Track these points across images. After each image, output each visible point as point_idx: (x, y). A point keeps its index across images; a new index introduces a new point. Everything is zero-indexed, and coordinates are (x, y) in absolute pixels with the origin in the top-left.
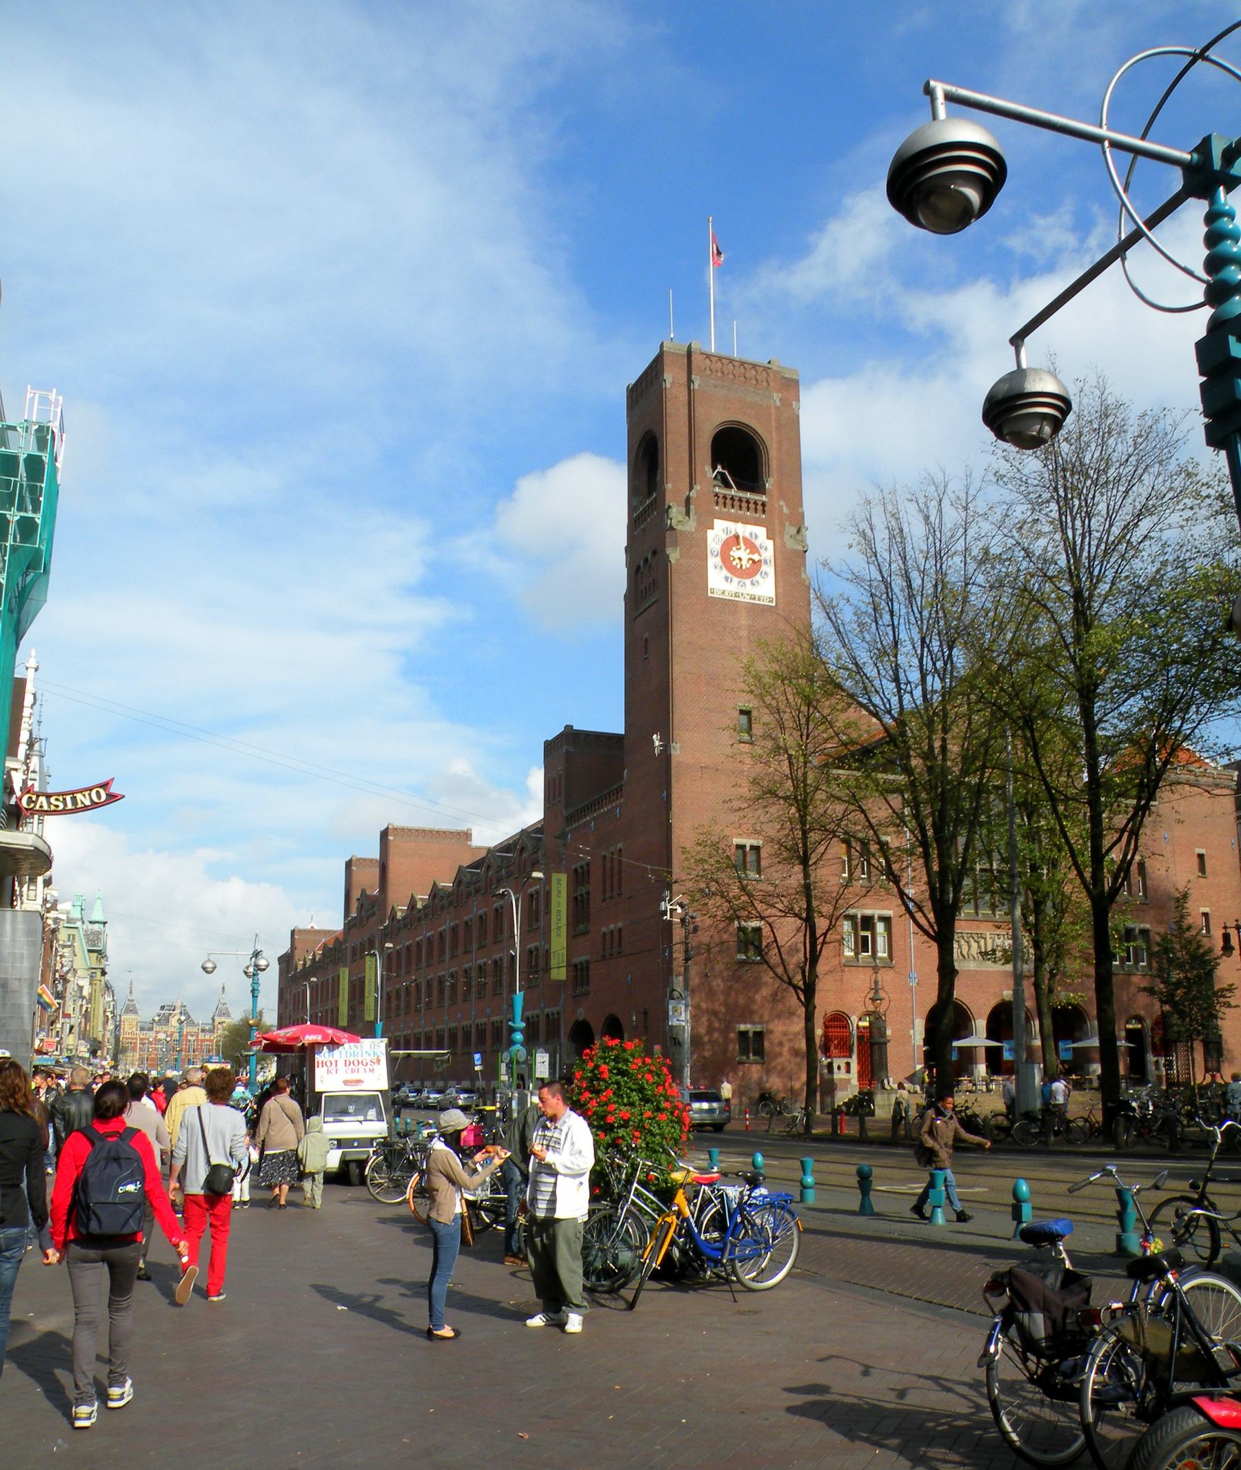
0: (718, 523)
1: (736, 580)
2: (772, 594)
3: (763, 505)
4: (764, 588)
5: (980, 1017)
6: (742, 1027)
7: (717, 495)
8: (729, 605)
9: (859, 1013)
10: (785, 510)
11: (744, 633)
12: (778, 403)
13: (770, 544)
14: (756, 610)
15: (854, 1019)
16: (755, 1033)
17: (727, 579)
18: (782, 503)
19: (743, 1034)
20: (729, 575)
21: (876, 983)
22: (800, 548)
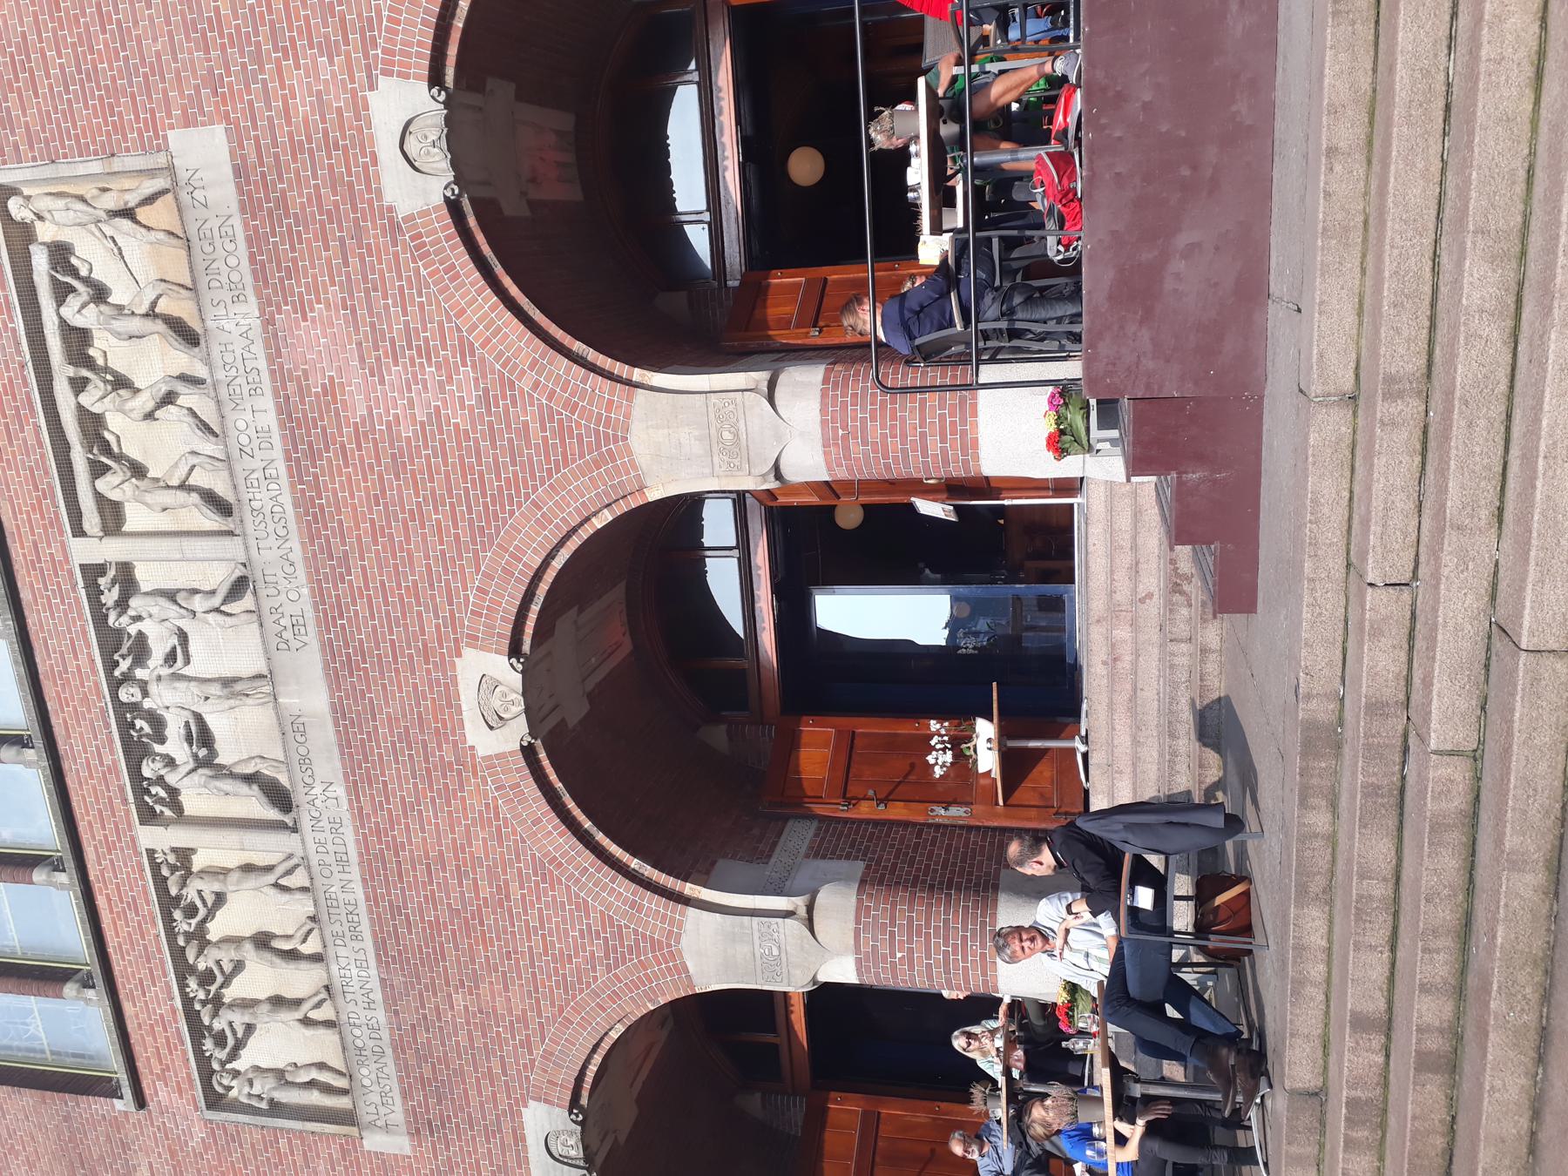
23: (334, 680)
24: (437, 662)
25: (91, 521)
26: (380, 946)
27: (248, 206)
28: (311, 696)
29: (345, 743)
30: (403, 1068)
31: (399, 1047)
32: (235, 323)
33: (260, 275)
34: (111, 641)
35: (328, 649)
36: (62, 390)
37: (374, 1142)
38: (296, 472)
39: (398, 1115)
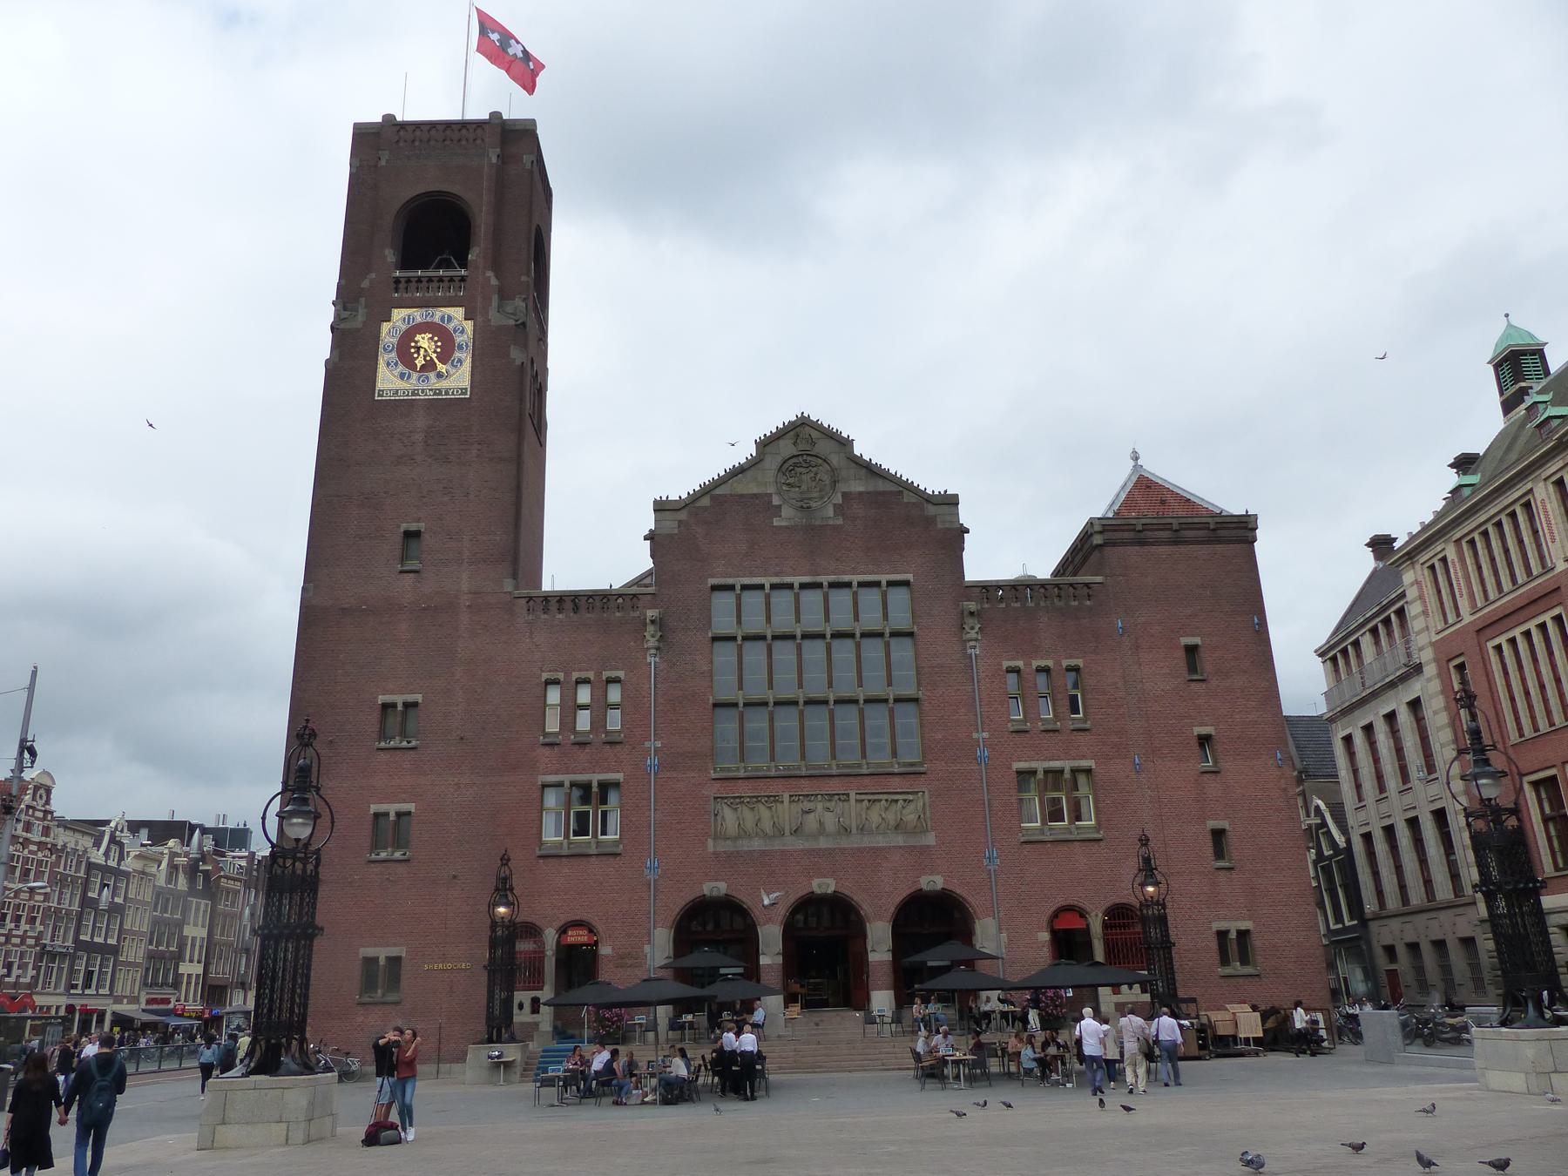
0: (398, 314)
2: (466, 383)
3: (463, 279)
4: (458, 378)
5: (769, 920)
6: (370, 952)
7: (397, 281)
8: (402, 407)
10: (494, 282)
11: (419, 437)
12: (494, 160)
14: (441, 407)
15: (550, 936)
16: (389, 959)
17: (402, 376)
18: (490, 274)
19: (371, 962)
20: (406, 371)
22: (512, 322)
24: (833, 874)
28: (823, 843)
32: (900, 840)
37: (710, 842)
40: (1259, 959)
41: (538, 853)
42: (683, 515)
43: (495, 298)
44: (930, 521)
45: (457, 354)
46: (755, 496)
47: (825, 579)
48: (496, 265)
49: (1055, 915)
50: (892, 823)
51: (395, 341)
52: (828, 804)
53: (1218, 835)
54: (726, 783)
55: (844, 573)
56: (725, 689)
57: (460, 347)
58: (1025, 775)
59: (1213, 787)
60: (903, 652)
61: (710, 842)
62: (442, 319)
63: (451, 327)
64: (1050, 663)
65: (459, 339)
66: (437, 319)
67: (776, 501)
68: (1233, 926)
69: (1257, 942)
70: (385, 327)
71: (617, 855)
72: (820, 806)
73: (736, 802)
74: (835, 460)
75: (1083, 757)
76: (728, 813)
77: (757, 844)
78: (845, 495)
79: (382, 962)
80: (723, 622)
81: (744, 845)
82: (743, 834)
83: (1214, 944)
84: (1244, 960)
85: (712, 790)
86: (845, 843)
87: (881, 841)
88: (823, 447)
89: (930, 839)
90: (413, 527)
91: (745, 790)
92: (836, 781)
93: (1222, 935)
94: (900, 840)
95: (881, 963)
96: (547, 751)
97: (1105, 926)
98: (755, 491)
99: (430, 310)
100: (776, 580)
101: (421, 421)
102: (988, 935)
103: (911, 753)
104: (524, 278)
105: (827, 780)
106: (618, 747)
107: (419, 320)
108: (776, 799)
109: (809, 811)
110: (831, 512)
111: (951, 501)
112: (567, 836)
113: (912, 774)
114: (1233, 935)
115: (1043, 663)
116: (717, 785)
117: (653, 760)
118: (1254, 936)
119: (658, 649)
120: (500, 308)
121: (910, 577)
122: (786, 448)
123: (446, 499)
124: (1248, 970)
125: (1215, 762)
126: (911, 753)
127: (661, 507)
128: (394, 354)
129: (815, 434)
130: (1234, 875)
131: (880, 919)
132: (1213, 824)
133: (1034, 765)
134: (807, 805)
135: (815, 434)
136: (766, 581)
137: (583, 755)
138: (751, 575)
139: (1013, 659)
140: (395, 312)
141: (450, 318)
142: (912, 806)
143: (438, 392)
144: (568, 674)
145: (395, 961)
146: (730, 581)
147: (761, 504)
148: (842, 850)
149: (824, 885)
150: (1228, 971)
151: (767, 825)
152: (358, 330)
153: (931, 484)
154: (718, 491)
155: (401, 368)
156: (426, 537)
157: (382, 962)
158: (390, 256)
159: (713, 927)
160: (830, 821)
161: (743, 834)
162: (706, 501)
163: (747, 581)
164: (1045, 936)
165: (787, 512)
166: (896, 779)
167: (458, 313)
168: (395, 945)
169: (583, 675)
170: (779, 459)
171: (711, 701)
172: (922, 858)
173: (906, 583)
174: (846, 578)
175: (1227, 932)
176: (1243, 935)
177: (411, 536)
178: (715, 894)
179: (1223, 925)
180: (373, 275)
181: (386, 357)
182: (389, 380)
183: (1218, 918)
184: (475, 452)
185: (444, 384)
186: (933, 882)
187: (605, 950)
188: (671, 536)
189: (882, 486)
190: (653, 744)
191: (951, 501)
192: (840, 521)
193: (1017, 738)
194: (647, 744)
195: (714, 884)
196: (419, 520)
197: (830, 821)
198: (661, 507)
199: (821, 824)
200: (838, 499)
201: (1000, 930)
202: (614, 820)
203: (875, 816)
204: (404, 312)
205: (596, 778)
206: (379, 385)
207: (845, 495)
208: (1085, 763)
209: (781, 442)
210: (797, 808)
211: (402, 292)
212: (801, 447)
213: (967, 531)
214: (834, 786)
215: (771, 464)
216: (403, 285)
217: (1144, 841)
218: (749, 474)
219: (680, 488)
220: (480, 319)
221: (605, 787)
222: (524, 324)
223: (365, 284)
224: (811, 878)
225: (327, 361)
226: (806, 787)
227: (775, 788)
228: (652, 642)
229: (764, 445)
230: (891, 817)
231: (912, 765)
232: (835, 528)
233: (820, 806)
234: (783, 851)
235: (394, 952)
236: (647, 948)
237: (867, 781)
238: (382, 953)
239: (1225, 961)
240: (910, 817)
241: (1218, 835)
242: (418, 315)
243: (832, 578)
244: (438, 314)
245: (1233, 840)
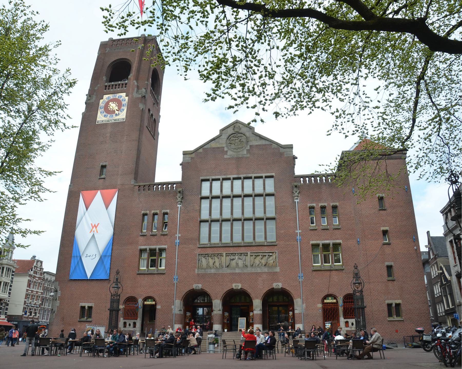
0: (105, 97)
1: (109, 115)
2: (124, 117)
3: (126, 84)
4: (122, 115)
6: (83, 304)
7: (106, 86)
8: (104, 125)
9: (143, 297)
10: (136, 84)
13: (127, 98)
14: (116, 124)
15: (140, 301)
17: (105, 116)
18: (135, 81)
19: (83, 308)
20: (106, 114)
21: (117, 279)
23: (239, 273)
24: (240, 282)
25: (251, 254)
26: (215, 274)
27: (274, 272)
28: (237, 271)
29: (233, 273)
30: (204, 274)
31: (206, 274)
32: (266, 270)
33: (269, 272)
34: (241, 253)
35: (241, 273)
36: (261, 254)
37: (196, 270)
38: (255, 273)
39: (199, 273)
40: (404, 314)
41: (137, 273)
42: (193, 155)
43: (136, 89)
44: (281, 154)
45: (122, 108)
46: (218, 148)
47: (242, 176)
48: (137, 79)
49: (325, 297)
50: (264, 264)
51: (104, 105)
52: (240, 257)
53: (389, 268)
54: (203, 249)
55: (249, 174)
56: (205, 215)
57: (124, 105)
58: (315, 246)
59: (388, 249)
60: (271, 201)
61: (196, 270)
62: (119, 97)
63: (121, 99)
64: (326, 204)
65: (123, 103)
66: (117, 97)
67: (226, 149)
68: (394, 302)
69: (403, 308)
70: (101, 101)
71: (163, 274)
72: (237, 257)
73: (206, 256)
74: (247, 134)
75: (338, 239)
76: (204, 260)
77: (213, 271)
78: (251, 146)
79: (86, 308)
80: (205, 192)
81: (209, 271)
82: (208, 267)
83: (386, 309)
84: (398, 315)
85: (199, 251)
86: (246, 271)
87: (259, 270)
88: (244, 130)
89: (278, 270)
90: (104, 164)
91: (209, 251)
92: (243, 248)
93: (389, 305)
94: (266, 270)
95: (257, 314)
96: (142, 238)
97: (344, 302)
98: (219, 146)
99: (115, 95)
100: (224, 177)
101: (109, 130)
102: (299, 306)
103: (272, 238)
104: (146, 82)
105: (240, 248)
106: (166, 236)
107: (112, 98)
108: (221, 255)
109: (233, 260)
110: (245, 152)
111: (290, 147)
112: (148, 267)
113: (272, 245)
114: (394, 305)
115: (323, 204)
116: (200, 250)
117: (177, 241)
118: (402, 306)
119: (181, 202)
120: (137, 91)
121: (273, 174)
122: (230, 131)
123: (115, 154)
124: (399, 319)
125: (389, 240)
126: (272, 238)
127: (185, 153)
128: (103, 109)
129: (241, 126)
130: (395, 282)
131: (257, 298)
132: (387, 263)
133: (318, 242)
134: (232, 257)
135: (241, 126)
136: (221, 177)
137: (154, 239)
138: (215, 175)
139: (311, 203)
140: (105, 96)
141: (121, 96)
142: (271, 258)
143: (115, 120)
144: (150, 211)
145: (90, 308)
146: (208, 178)
147: (221, 150)
148: (244, 274)
149: (237, 286)
150: (391, 319)
151: (217, 264)
152: (93, 103)
153: (283, 142)
154: (205, 147)
155: (105, 113)
156: (108, 167)
157: (86, 308)
158: (104, 78)
159: (194, 300)
160: (240, 263)
161: (208, 267)
162: (201, 150)
163: (214, 177)
164: (320, 305)
165: (230, 153)
166: (265, 248)
167: (124, 94)
168: (91, 302)
169: (155, 211)
170: (228, 135)
171: (199, 220)
172: (274, 276)
173: (272, 177)
174: (250, 175)
175: (391, 304)
176: (398, 305)
177: (103, 167)
178: (197, 288)
179: (390, 302)
180: (99, 85)
181: (101, 110)
182: (101, 117)
183: (388, 299)
184: (125, 138)
185: (118, 117)
186: (278, 285)
187: (158, 307)
188: (188, 163)
189: (263, 142)
190: (178, 235)
191: (290, 147)
192: (249, 155)
193: (312, 232)
194: (176, 235)
195: (197, 285)
196: (106, 162)
197: (240, 263)
198: (185, 153)
199: (237, 264)
200: (248, 147)
201: (303, 303)
202: (164, 262)
203: (257, 261)
204: (107, 96)
205: (158, 247)
206: (98, 119)
207: (251, 146)
208: (338, 241)
209: (229, 129)
210: (228, 258)
211: (108, 89)
212: (236, 130)
213: (297, 158)
214: (242, 250)
215: (224, 137)
216: (107, 88)
217: (356, 267)
218: (216, 140)
219: (192, 148)
220: (130, 96)
221: (161, 250)
222: (144, 96)
223: (96, 88)
224: (232, 283)
225: (83, 113)
226: (232, 250)
227: (220, 251)
228: (179, 199)
229: (222, 130)
230: (263, 261)
231: (272, 242)
232: (246, 158)
233: (237, 257)
234: (222, 273)
235: (90, 305)
236: (173, 307)
237: (254, 248)
238: (86, 305)
239: (390, 315)
240: (271, 261)
241: (389, 268)
242: (111, 96)
243: (245, 175)
244: (118, 95)
245: (395, 269)
